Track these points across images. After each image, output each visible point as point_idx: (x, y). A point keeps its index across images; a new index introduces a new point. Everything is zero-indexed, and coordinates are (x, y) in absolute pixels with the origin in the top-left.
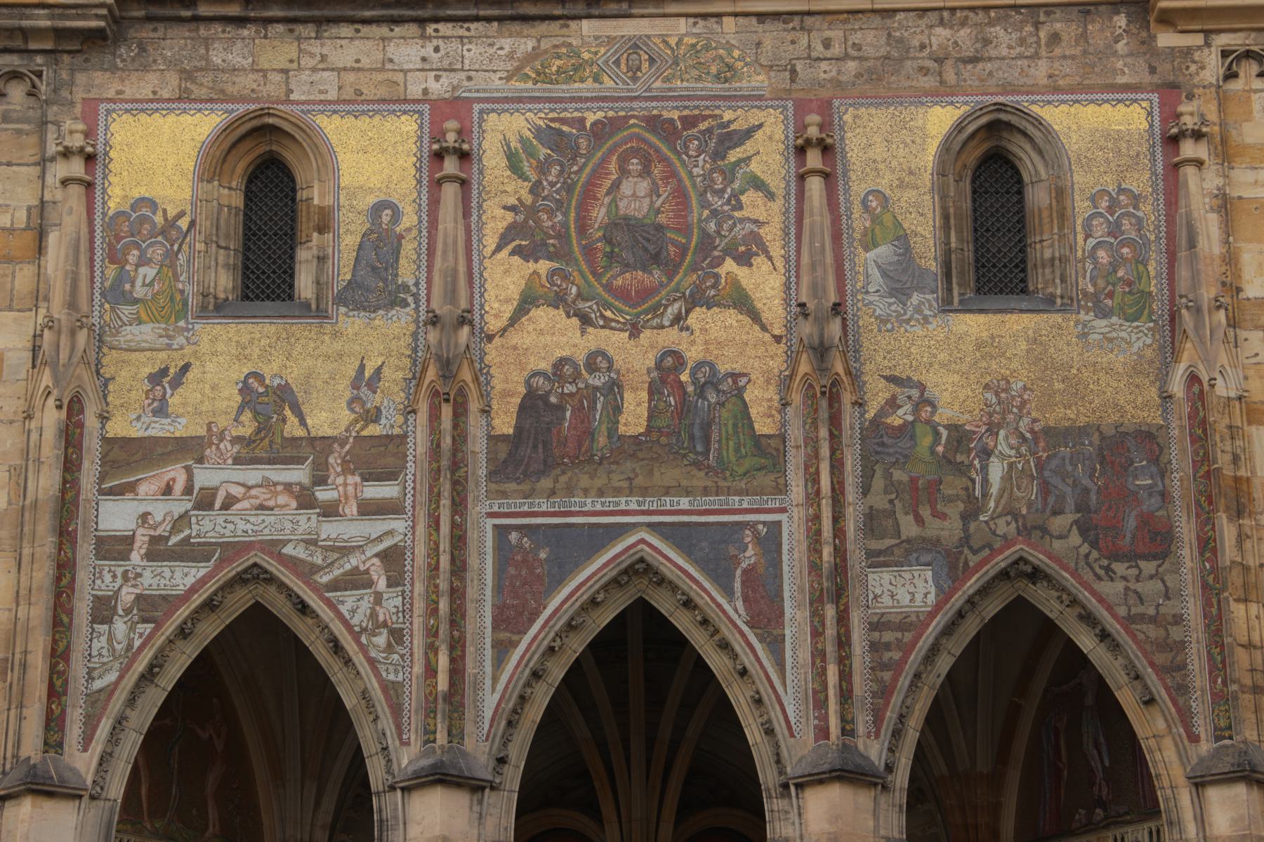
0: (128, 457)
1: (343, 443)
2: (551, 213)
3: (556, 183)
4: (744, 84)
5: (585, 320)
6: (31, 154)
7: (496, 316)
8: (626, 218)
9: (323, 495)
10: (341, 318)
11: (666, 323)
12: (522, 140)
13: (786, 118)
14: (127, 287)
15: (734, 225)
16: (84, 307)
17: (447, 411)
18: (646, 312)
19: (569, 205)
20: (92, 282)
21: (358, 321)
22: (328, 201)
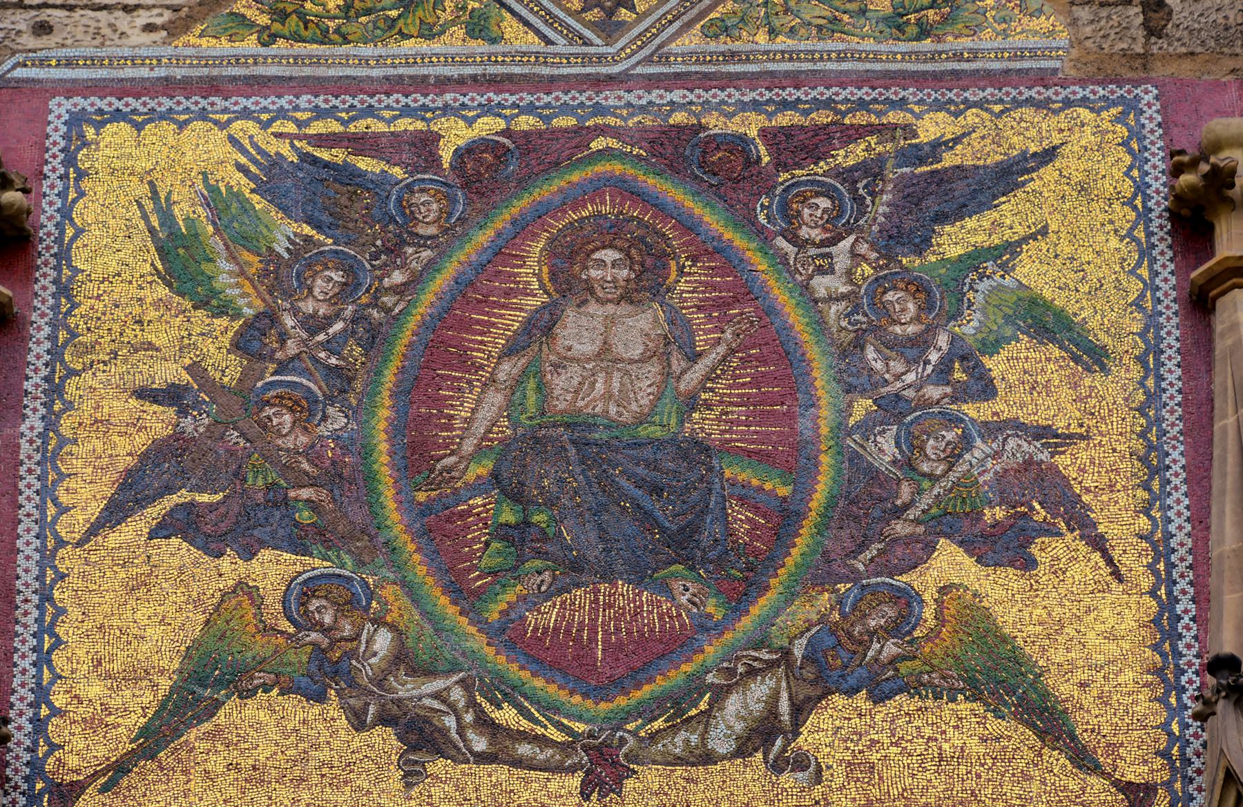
2: (306, 409)
3: (329, 320)
4: (987, 40)
5: (422, 738)
7: (92, 724)
8: (576, 424)
11: (722, 746)
12: (217, 201)
13: (1136, 133)
15: (966, 442)
18: (647, 712)
19: (371, 392)
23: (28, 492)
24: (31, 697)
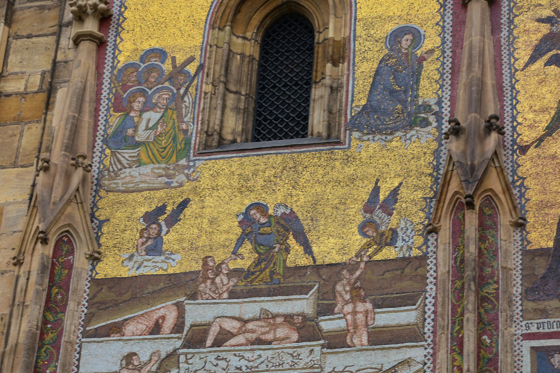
0: (116, 298)
1: (351, 267)
6: (50, 25)
7: (530, 127)
9: (328, 325)
10: (354, 143)
14: (130, 131)
16: (83, 149)
17: (471, 220)
20: (95, 130)
21: (373, 144)
22: (345, 33)
23: (505, 55)
24: (511, 120)
